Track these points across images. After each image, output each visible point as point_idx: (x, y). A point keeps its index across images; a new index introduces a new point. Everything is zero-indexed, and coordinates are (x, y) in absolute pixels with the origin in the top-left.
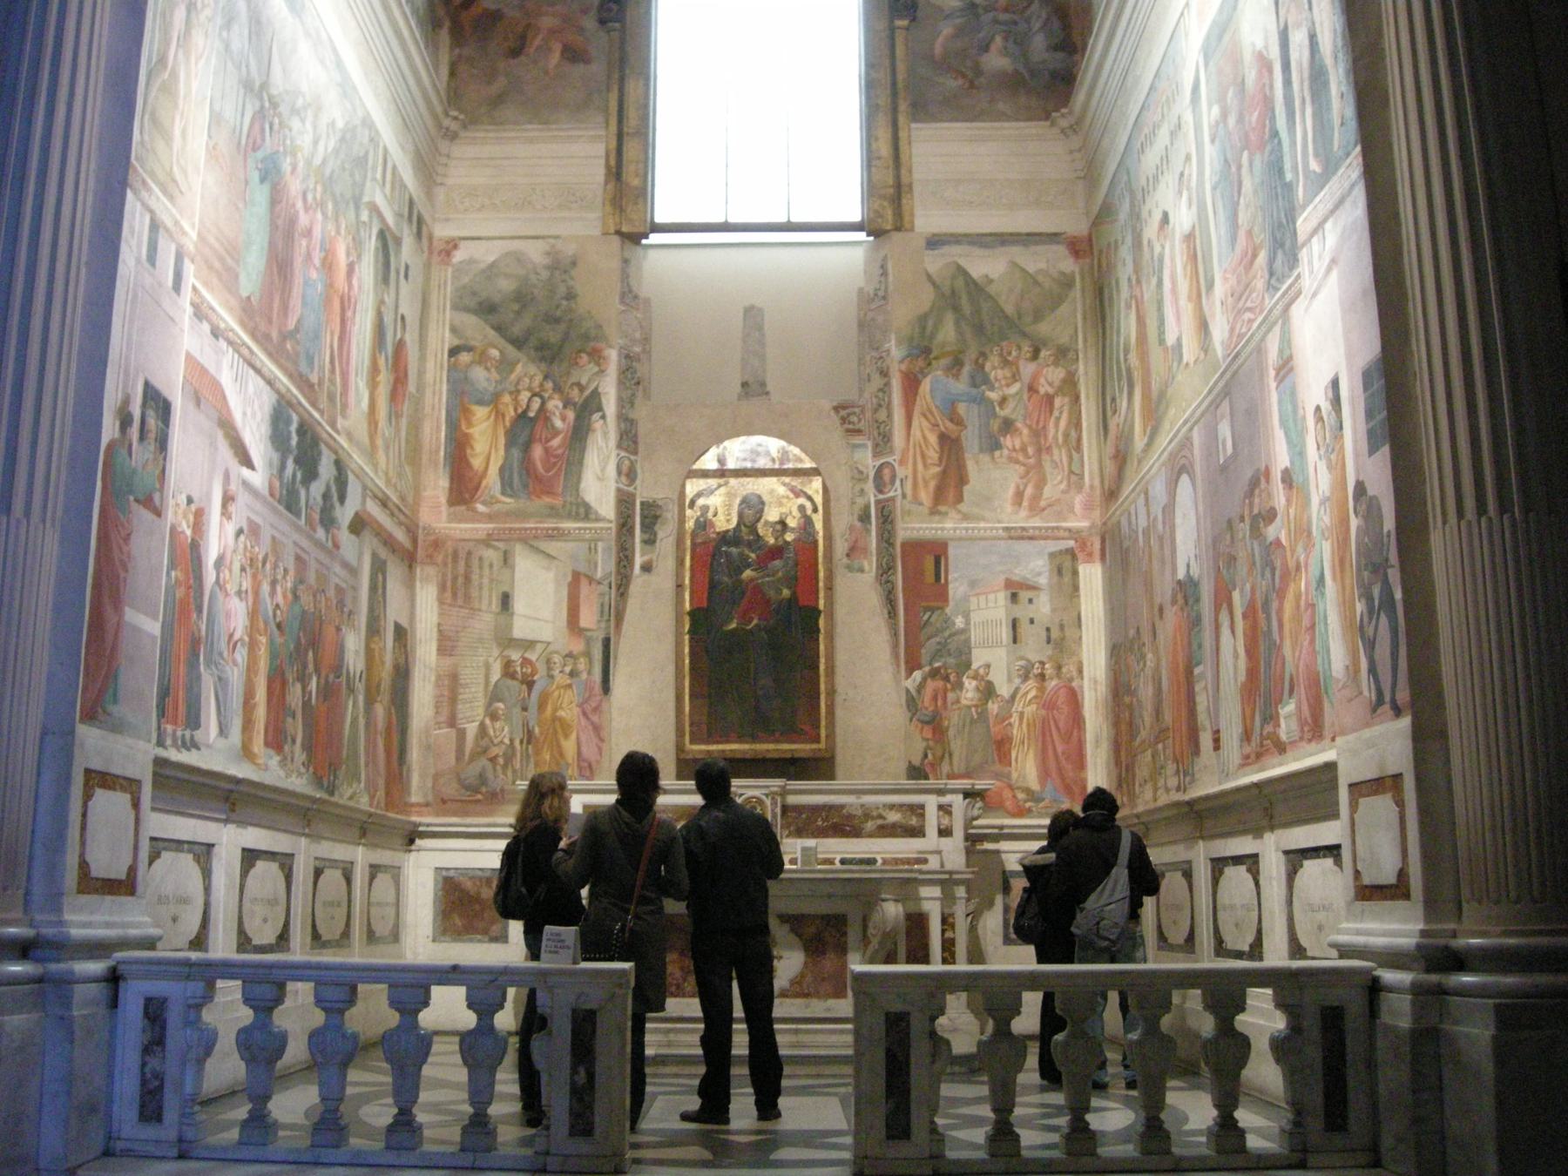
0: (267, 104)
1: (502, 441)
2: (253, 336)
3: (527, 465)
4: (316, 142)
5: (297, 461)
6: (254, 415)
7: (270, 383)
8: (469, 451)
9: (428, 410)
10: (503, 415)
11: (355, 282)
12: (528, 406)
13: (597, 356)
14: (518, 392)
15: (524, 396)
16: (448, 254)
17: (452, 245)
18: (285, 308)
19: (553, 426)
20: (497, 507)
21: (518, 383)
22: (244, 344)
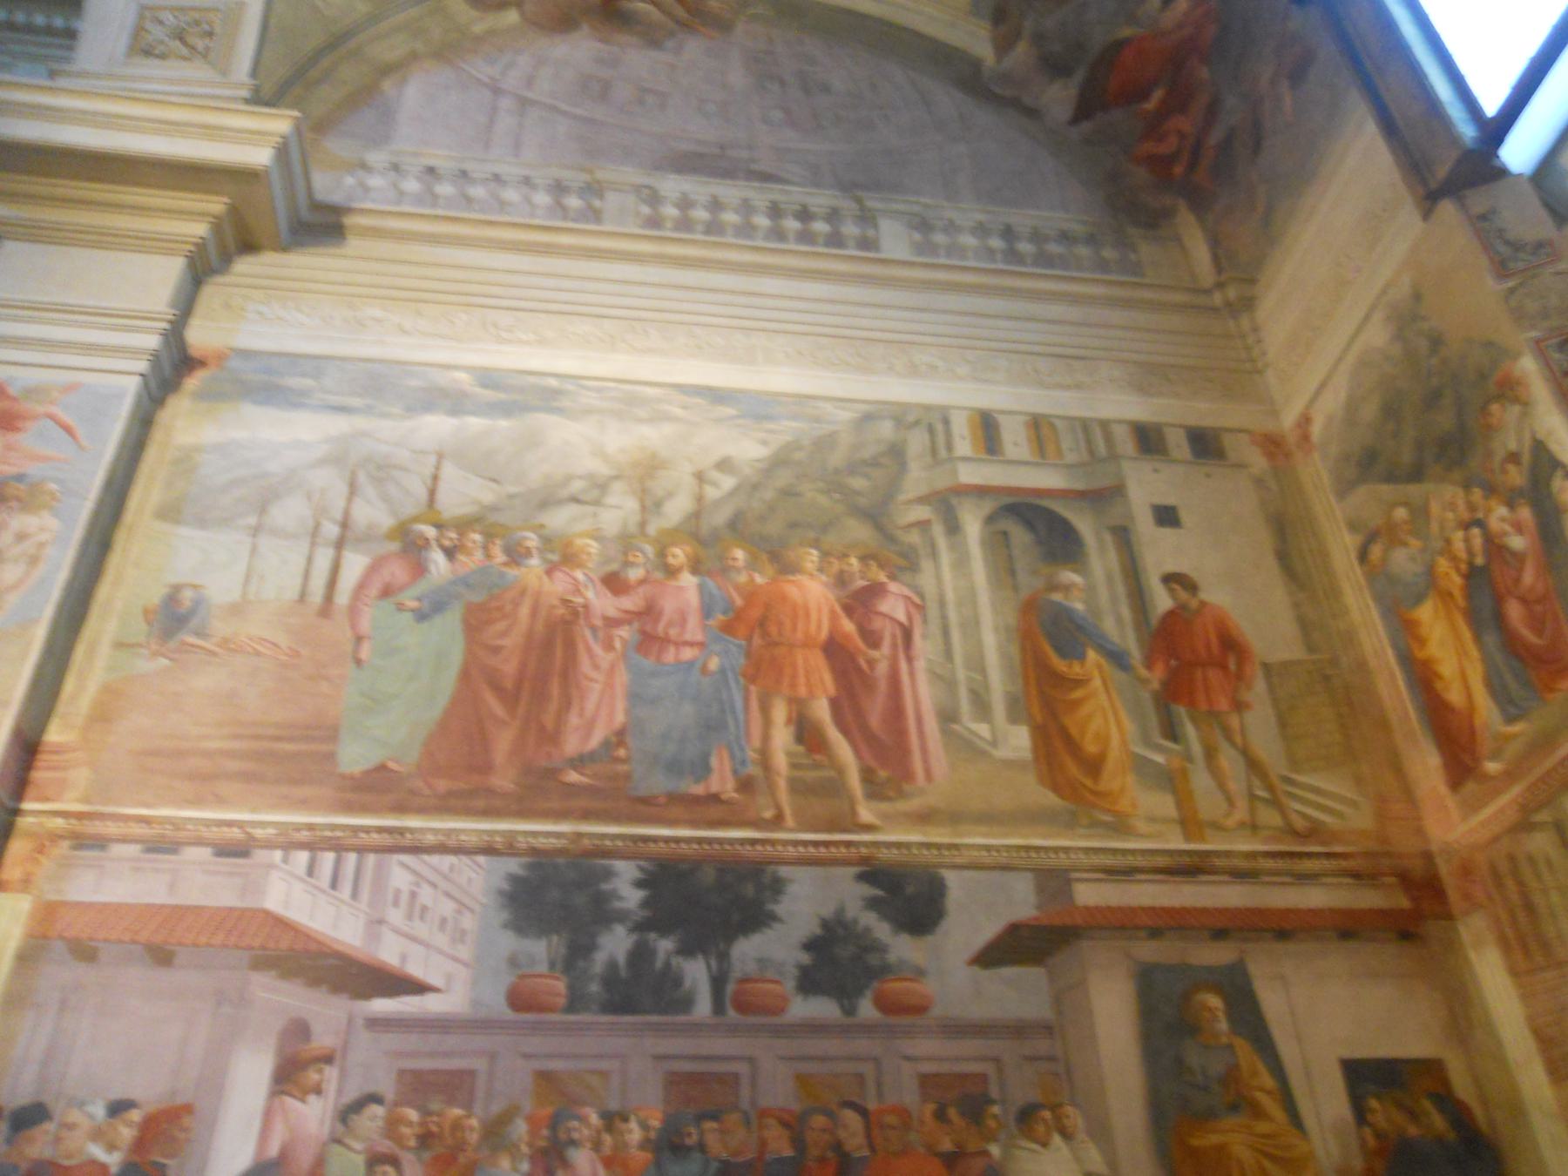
0: (430, 532)
1: (1467, 635)
2: (400, 809)
3: (1512, 644)
4: (651, 505)
5: (641, 927)
6: (417, 910)
7: (489, 850)
8: (1439, 685)
9: (1373, 663)
10: (1450, 594)
11: (893, 606)
12: (1470, 552)
13: (1509, 390)
14: (1448, 541)
15: (1459, 545)
16: (1306, 437)
17: (1305, 421)
18: (552, 737)
19: (1514, 554)
20: (1513, 750)
21: (1442, 528)
22: (356, 830)
